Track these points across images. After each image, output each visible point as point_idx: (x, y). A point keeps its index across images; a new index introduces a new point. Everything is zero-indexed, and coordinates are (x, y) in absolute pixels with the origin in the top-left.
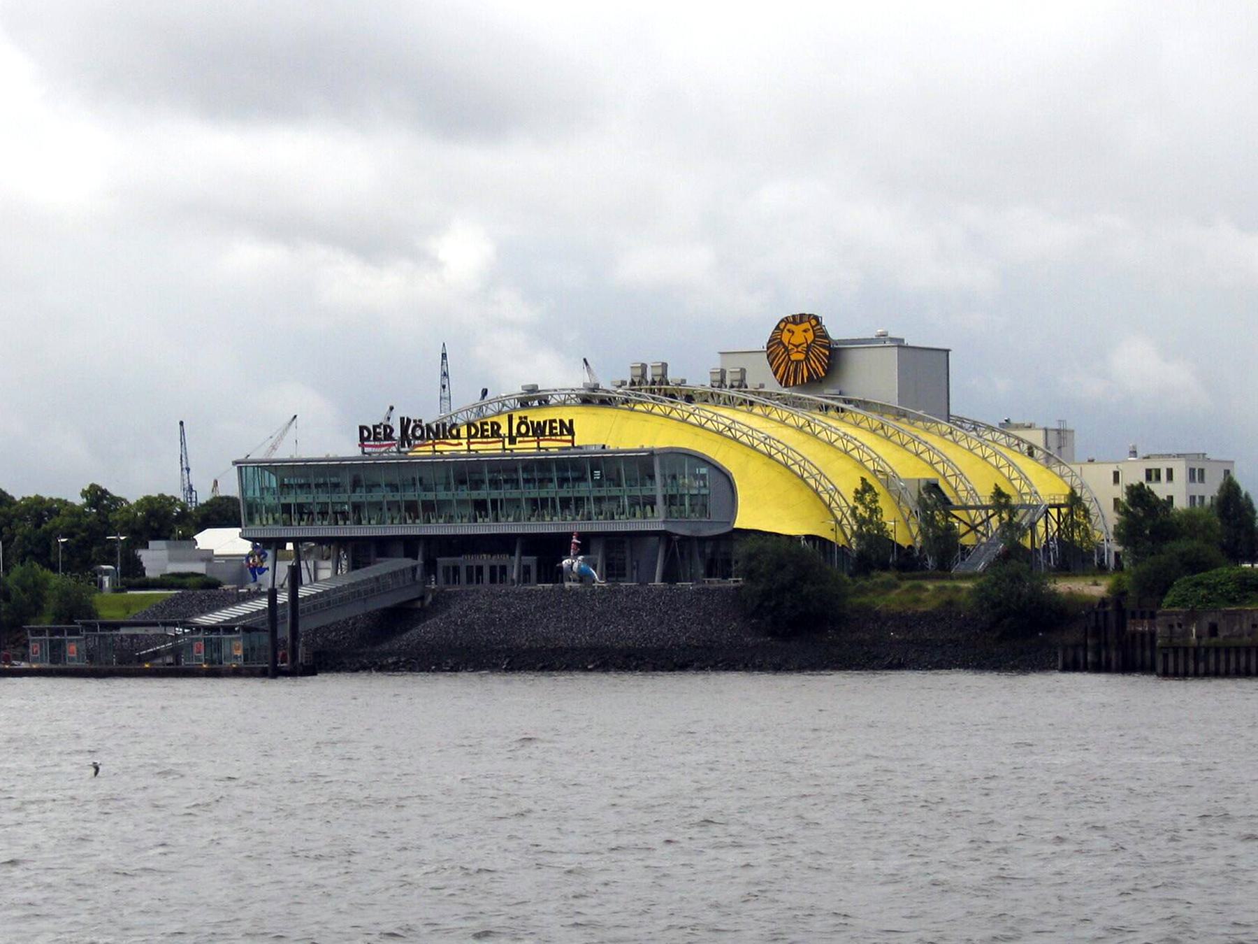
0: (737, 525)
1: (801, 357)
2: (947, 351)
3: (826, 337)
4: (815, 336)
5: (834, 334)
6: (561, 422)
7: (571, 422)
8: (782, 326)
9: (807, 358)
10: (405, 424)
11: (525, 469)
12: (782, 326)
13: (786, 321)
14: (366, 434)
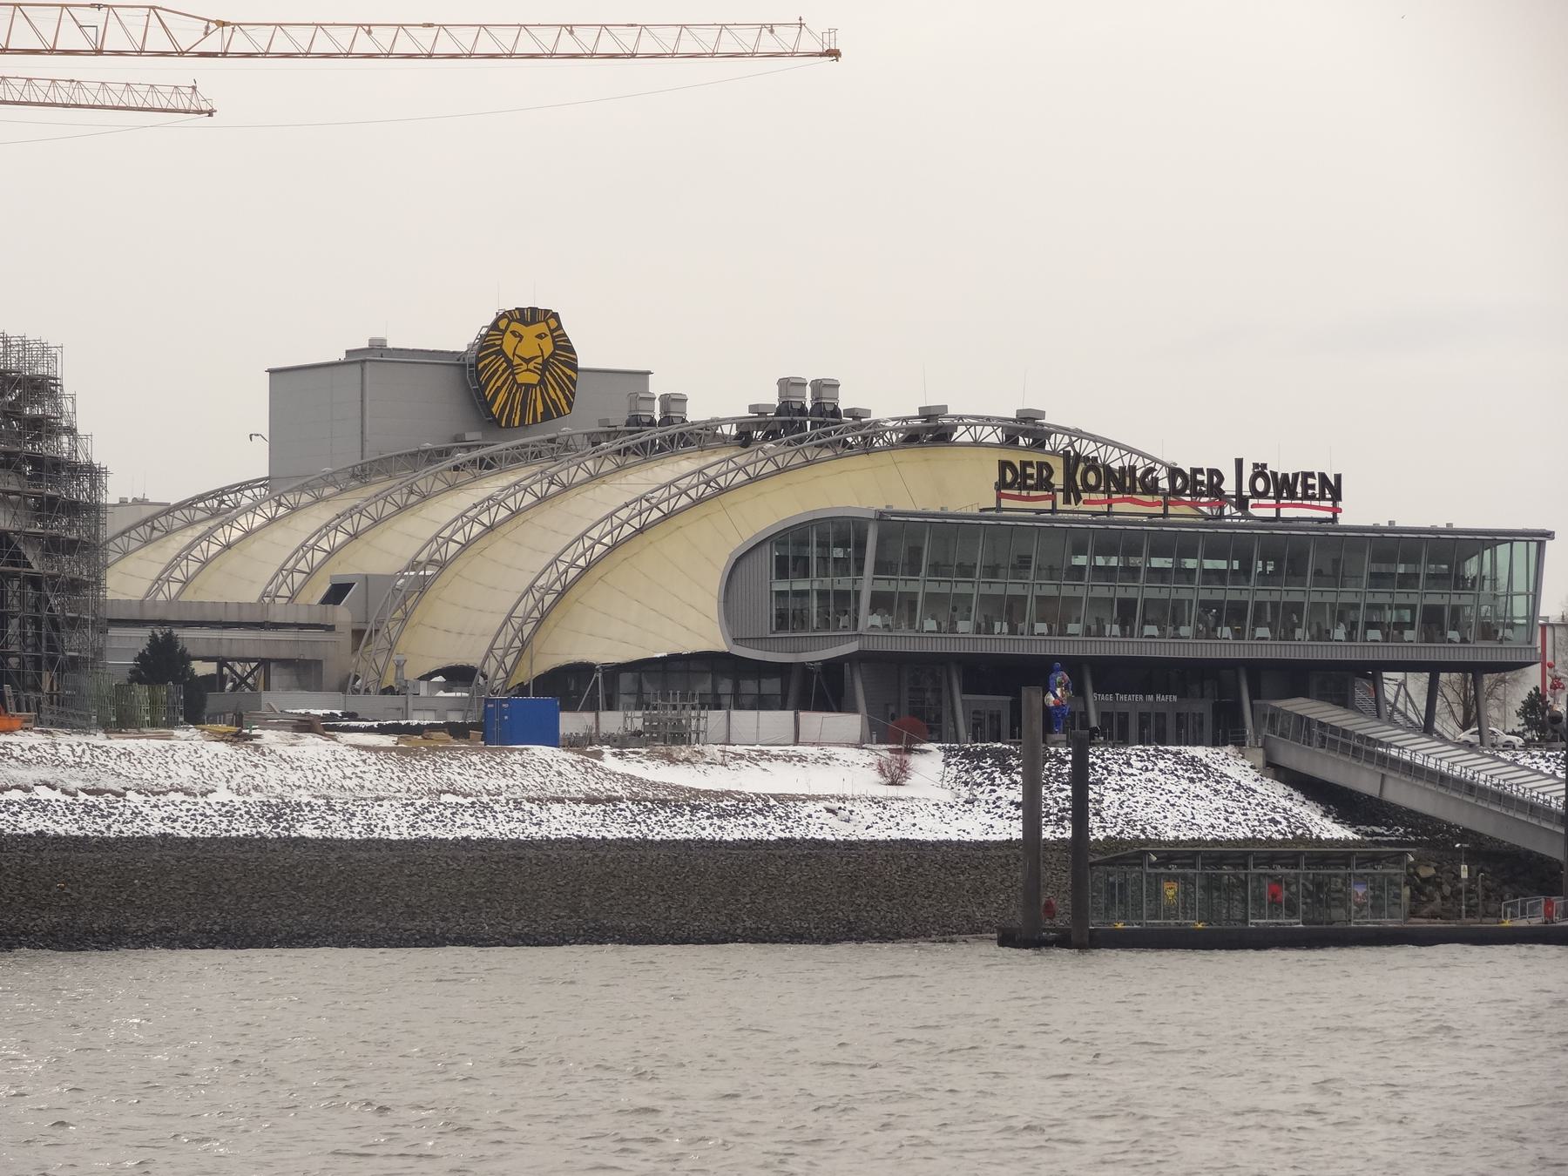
1: (533, 379)
3: (571, 350)
4: (556, 347)
6: (1323, 477)
7: (1338, 478)
8: (503, 324)
9: (542, 382)
12: (503, 324)
13: (507, 316)
14: (1009, 476)
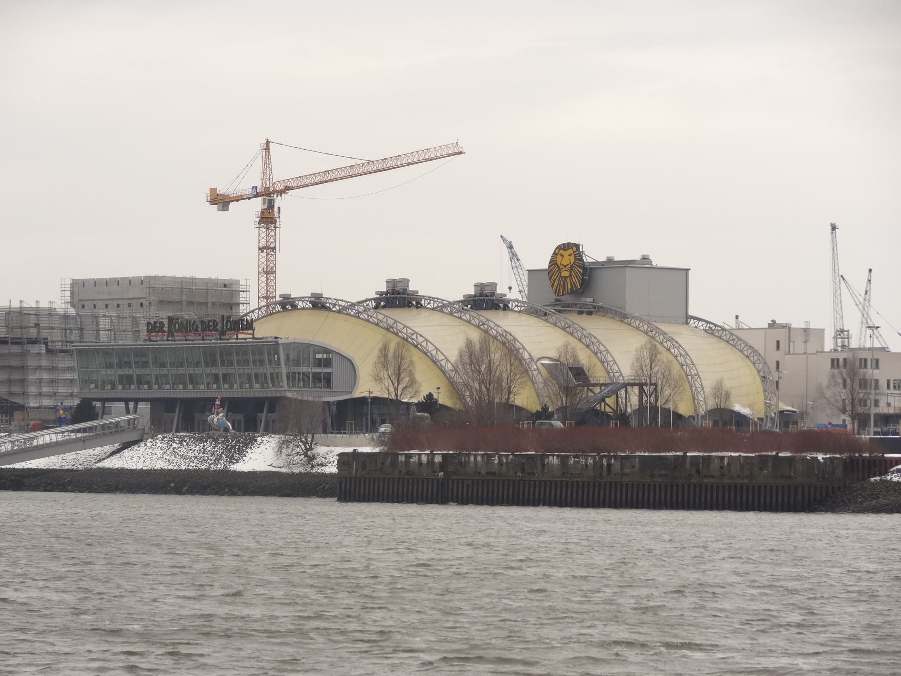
0: (358, 393)
2: (687, 270)
4: (576, 259)
5: (587, 260)
9: (570, 275)
10: (170, 319)
11: (237, 354)
